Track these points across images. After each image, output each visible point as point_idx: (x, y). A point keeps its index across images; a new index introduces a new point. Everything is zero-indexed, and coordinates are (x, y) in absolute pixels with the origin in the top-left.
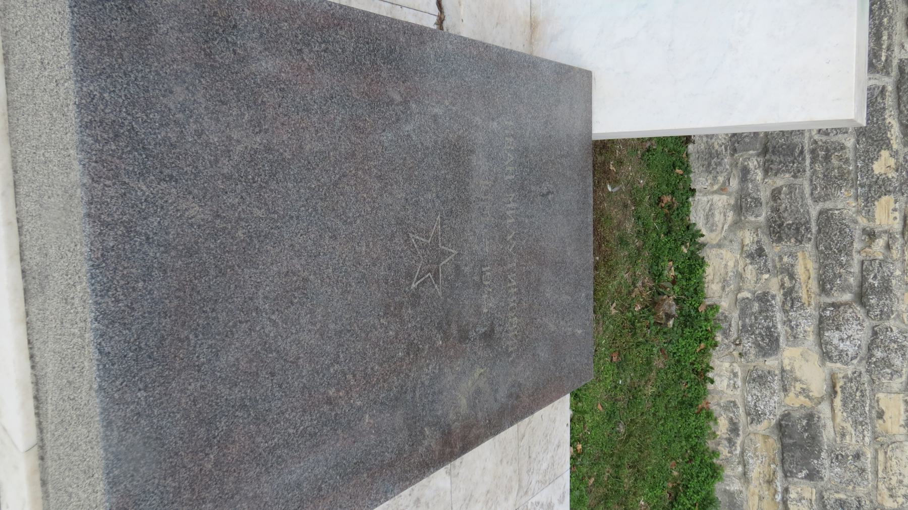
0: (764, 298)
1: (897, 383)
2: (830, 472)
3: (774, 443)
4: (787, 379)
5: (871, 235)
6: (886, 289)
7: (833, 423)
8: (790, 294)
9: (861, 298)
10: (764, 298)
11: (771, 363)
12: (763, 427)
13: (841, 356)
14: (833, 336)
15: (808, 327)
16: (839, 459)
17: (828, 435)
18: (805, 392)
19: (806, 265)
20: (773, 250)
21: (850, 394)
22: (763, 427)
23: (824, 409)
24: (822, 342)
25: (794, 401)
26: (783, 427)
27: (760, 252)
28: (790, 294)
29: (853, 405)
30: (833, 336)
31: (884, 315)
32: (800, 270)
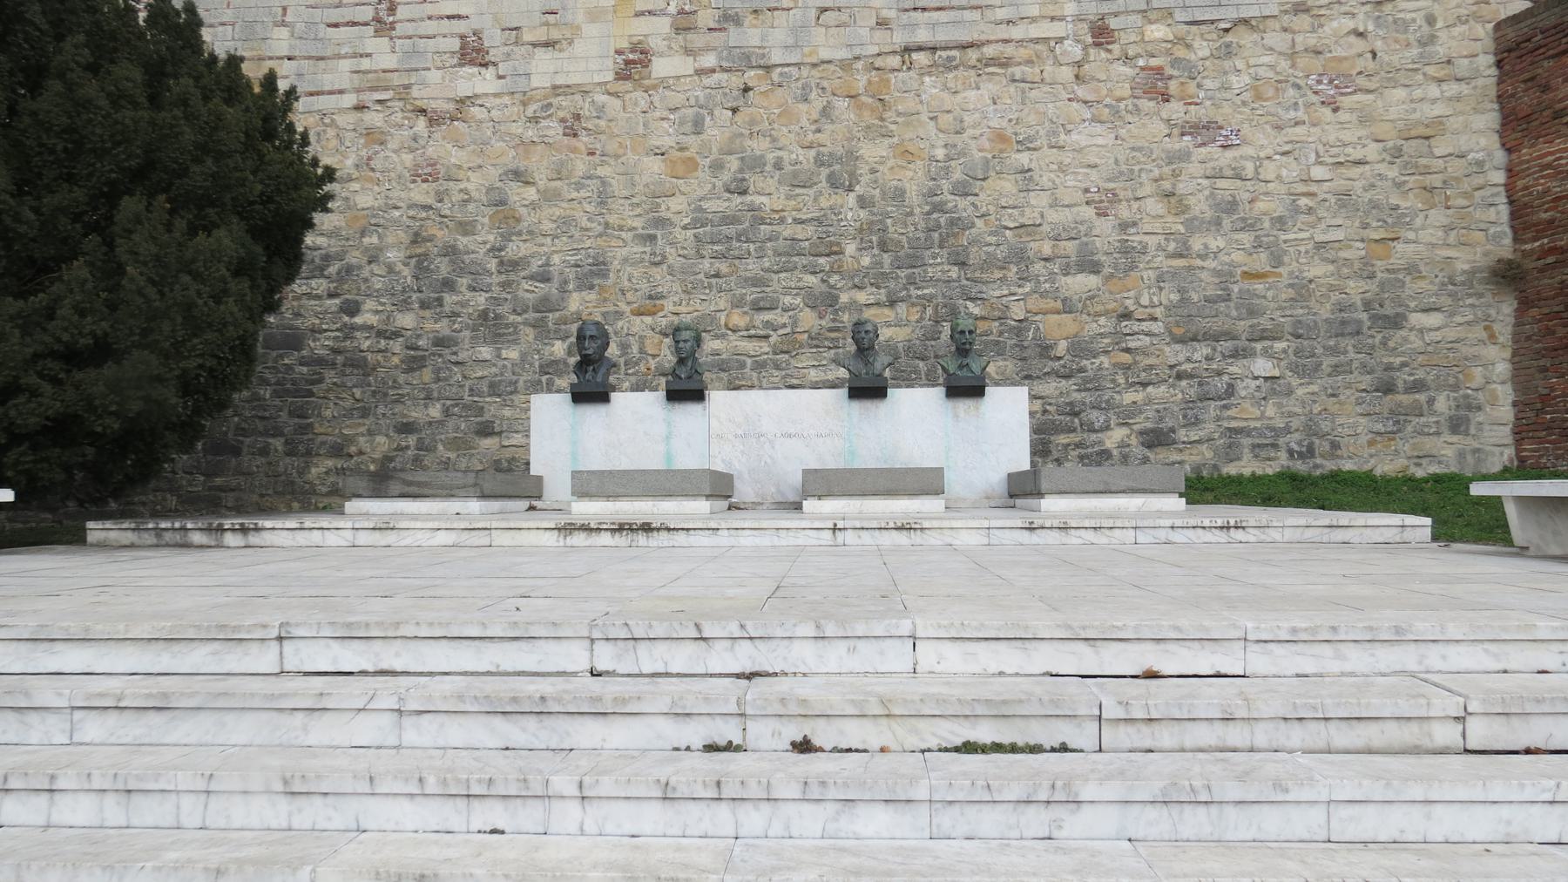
0: (1081, 458)
1: (1117, 397)
2: (1169, 423)
3: (1158, 450)
4: (1122, 445)
5: (1045, 412)
6: (1071, 404)
7: (1143, 422)
8: (1078, 446)
9: (1076, 414)
10: (1081, 458)
11: (1115, 452)
12: (1151, 456)
13: (1107, 421)
14: (1097, 425)
15: (1094, 437)
16: (1161, 419)
17: (1149, 425)
18: (1128, 436)
19: (1063, 439)
20: (1055, 455)
21: (1126, 416)
22: (1151, 456)
23: (1135, 427)
24: (1101, 430)
25: (1134, 441)
26: (1149, 447)
27: (1057, 460)
28: (1078, 446)
29: (1132, 415)
30: (1097, 425)
31: (1084, 404)
32: (1066, 441)
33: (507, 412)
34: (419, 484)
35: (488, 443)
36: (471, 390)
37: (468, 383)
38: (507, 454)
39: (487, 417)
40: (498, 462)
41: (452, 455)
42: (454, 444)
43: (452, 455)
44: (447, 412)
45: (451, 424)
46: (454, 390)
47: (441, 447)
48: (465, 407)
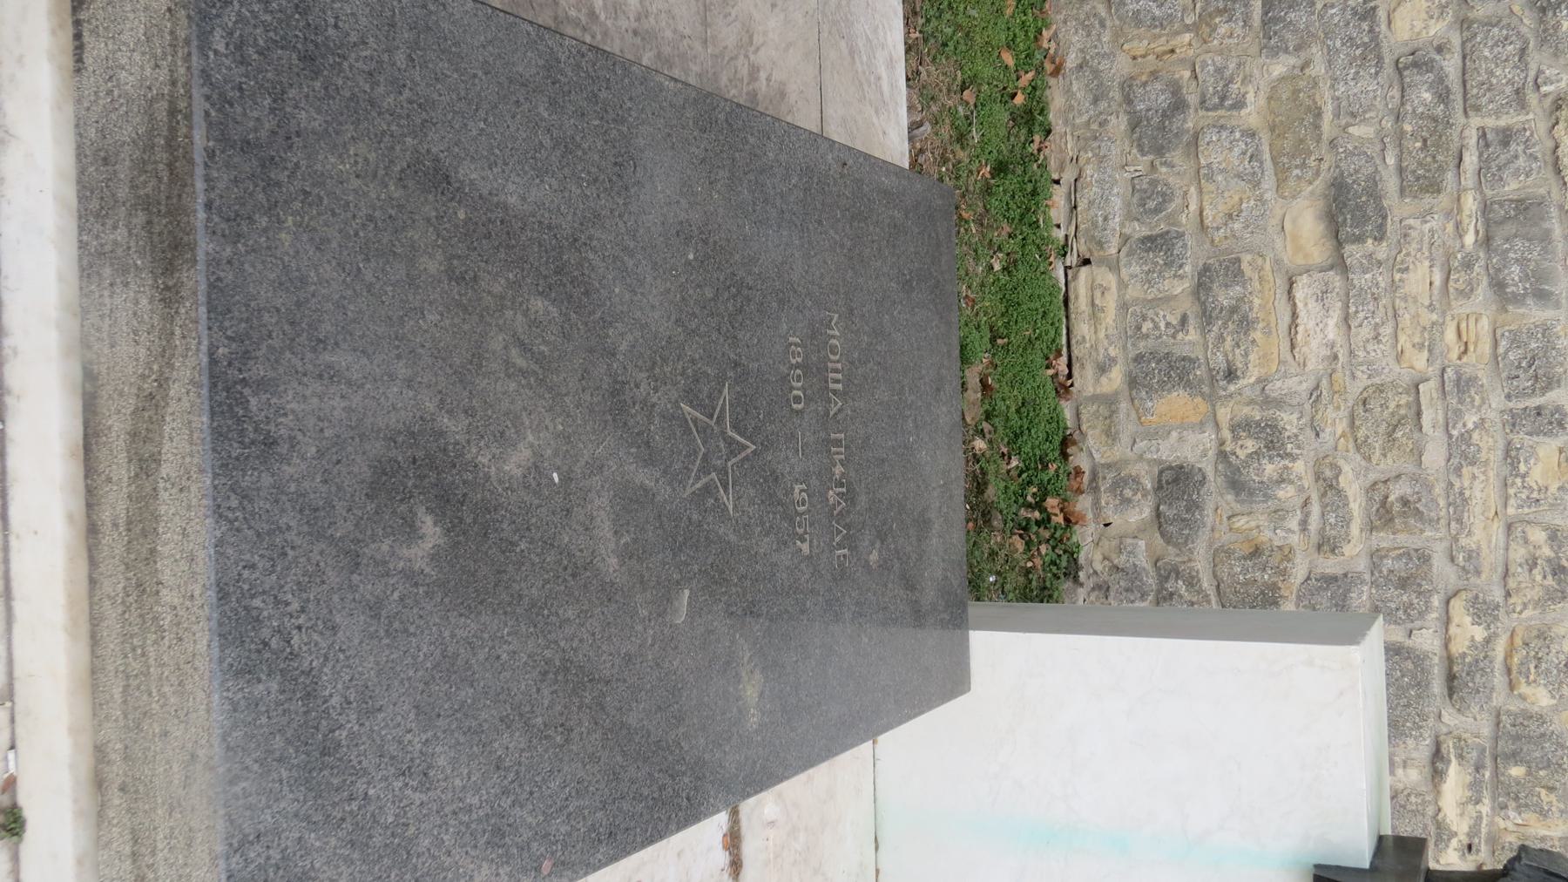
33: (1421, 278)
34: (142, 523)
35: (1304, 224)
36: (1506, 137)
37: (1534, 119)
38: (1264, 299)
39: (1399, 208)
40: (1233, 271)
41: (1252, 115)
42: (1296, 118)
43: (1252, 115)
44: (1418, 61)
45: (1372, 88)
46: (1504, 74)
47: (1279, 67)
48: (1436, 130)
